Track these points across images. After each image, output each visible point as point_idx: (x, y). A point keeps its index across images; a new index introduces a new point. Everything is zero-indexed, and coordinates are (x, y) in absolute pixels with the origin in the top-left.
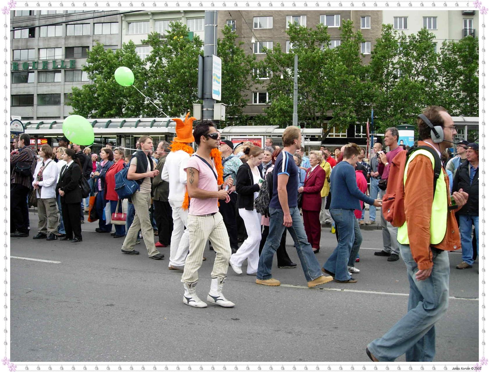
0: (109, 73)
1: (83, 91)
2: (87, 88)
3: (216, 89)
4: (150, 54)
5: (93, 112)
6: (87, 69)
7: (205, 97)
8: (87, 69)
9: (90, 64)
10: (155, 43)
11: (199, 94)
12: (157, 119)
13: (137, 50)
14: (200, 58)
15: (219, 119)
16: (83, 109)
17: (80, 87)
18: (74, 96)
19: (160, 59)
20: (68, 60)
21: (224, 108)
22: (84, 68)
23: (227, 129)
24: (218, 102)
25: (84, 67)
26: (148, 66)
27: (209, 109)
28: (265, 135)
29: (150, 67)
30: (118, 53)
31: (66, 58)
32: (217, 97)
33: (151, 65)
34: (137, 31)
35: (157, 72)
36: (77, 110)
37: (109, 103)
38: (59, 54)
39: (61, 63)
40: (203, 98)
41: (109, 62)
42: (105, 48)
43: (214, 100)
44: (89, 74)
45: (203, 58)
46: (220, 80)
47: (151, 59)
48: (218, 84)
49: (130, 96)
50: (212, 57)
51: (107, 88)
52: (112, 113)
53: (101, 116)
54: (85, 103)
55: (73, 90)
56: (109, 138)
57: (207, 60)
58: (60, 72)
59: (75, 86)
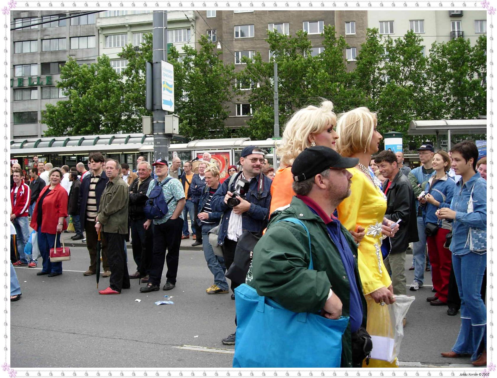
0: (83, 88)
1: (57, 108)
2: (61, 105)
3: (167, 99)
4: (125, 67)
5: (68, 129)
6: (61, 85)
7: (155, 110)
8: (61, 85)
9: (64, 80)
10: (131, 56)
11: (148, 105)
12: (132, 135)
13: (112, 64)
14: (148, 65)
15: (171, 133)
16: (58, 126)
17: (54, 103)
18: (48, 114)
19: (137, 72)
20: (44, 76)
21: (177, 120)
22: (57, 84)
23: (192, 144)
24: (169, 113)
25: (58, 82)
26: (124, 80)
27: (159, 122)
28: (234, 148)
29: (127, 81)
30: (93, 68)
31: (43, 73)
32: (169, 107)
33: (127, 78)
34: (115, 45)
35: (133, 86)
36: (52, 128)
37: (85, 119)
38: (35, 71)
39: (37, 80)
40: (153, 109)
41: (83, 77)
42: (78, 63)
43: (165, 111)
44: (63, 90)
45: (152, 64)
46: (173, 89)
47: (127, 73)
48: (170, 94)
49: (106, 111)
50: (160, 63)
51: (82, 103)
52: (87, 129)
53: (77, 133)
54: (59, 120)
55: (47, 107)
56: (84, 156)
57: (155, 66)
58: (36, 89)
59: (48, 104)
